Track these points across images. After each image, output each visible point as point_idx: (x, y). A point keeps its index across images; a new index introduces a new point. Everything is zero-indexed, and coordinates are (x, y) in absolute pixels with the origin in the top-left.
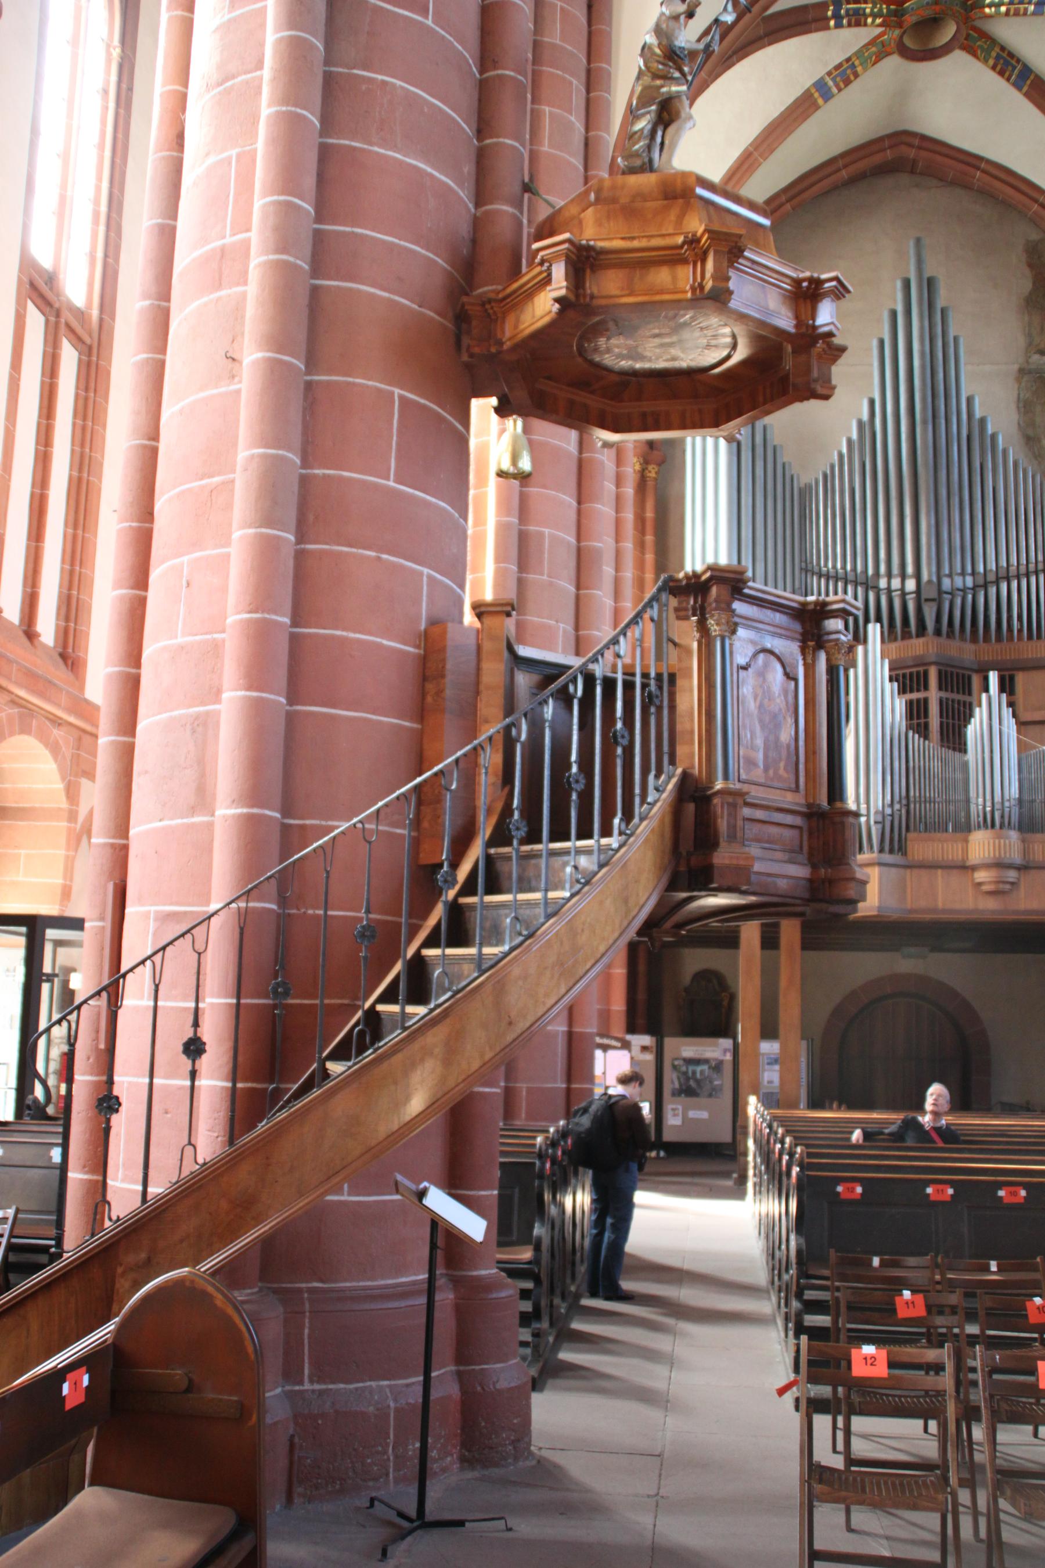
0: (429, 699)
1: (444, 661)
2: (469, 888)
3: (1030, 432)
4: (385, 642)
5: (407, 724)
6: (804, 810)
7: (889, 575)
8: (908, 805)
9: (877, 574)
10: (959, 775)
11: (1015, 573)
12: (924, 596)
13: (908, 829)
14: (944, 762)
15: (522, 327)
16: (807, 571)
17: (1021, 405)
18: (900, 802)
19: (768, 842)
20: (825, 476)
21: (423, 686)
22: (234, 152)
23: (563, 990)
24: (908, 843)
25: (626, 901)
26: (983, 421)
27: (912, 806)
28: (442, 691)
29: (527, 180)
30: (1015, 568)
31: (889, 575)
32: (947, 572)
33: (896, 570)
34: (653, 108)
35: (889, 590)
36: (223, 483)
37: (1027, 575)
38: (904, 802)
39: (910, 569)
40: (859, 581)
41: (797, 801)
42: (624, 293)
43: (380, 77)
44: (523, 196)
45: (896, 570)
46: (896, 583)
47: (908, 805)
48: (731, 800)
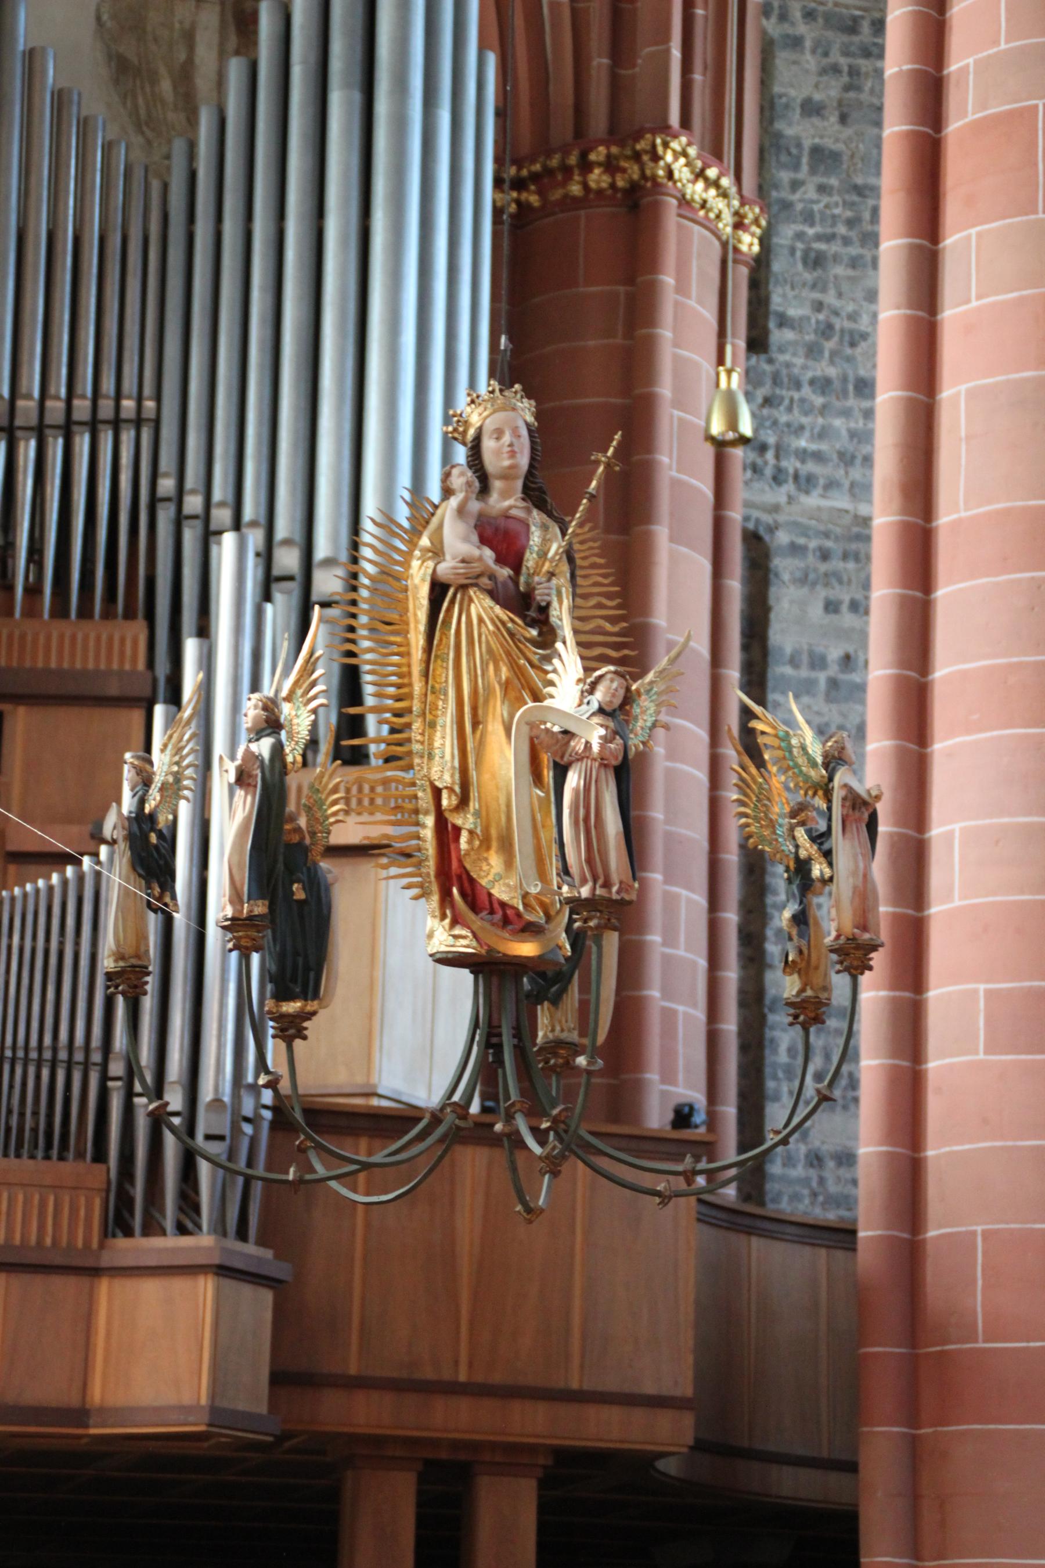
11: (34, 421)
30: (33, 405)
37: (68, 431)
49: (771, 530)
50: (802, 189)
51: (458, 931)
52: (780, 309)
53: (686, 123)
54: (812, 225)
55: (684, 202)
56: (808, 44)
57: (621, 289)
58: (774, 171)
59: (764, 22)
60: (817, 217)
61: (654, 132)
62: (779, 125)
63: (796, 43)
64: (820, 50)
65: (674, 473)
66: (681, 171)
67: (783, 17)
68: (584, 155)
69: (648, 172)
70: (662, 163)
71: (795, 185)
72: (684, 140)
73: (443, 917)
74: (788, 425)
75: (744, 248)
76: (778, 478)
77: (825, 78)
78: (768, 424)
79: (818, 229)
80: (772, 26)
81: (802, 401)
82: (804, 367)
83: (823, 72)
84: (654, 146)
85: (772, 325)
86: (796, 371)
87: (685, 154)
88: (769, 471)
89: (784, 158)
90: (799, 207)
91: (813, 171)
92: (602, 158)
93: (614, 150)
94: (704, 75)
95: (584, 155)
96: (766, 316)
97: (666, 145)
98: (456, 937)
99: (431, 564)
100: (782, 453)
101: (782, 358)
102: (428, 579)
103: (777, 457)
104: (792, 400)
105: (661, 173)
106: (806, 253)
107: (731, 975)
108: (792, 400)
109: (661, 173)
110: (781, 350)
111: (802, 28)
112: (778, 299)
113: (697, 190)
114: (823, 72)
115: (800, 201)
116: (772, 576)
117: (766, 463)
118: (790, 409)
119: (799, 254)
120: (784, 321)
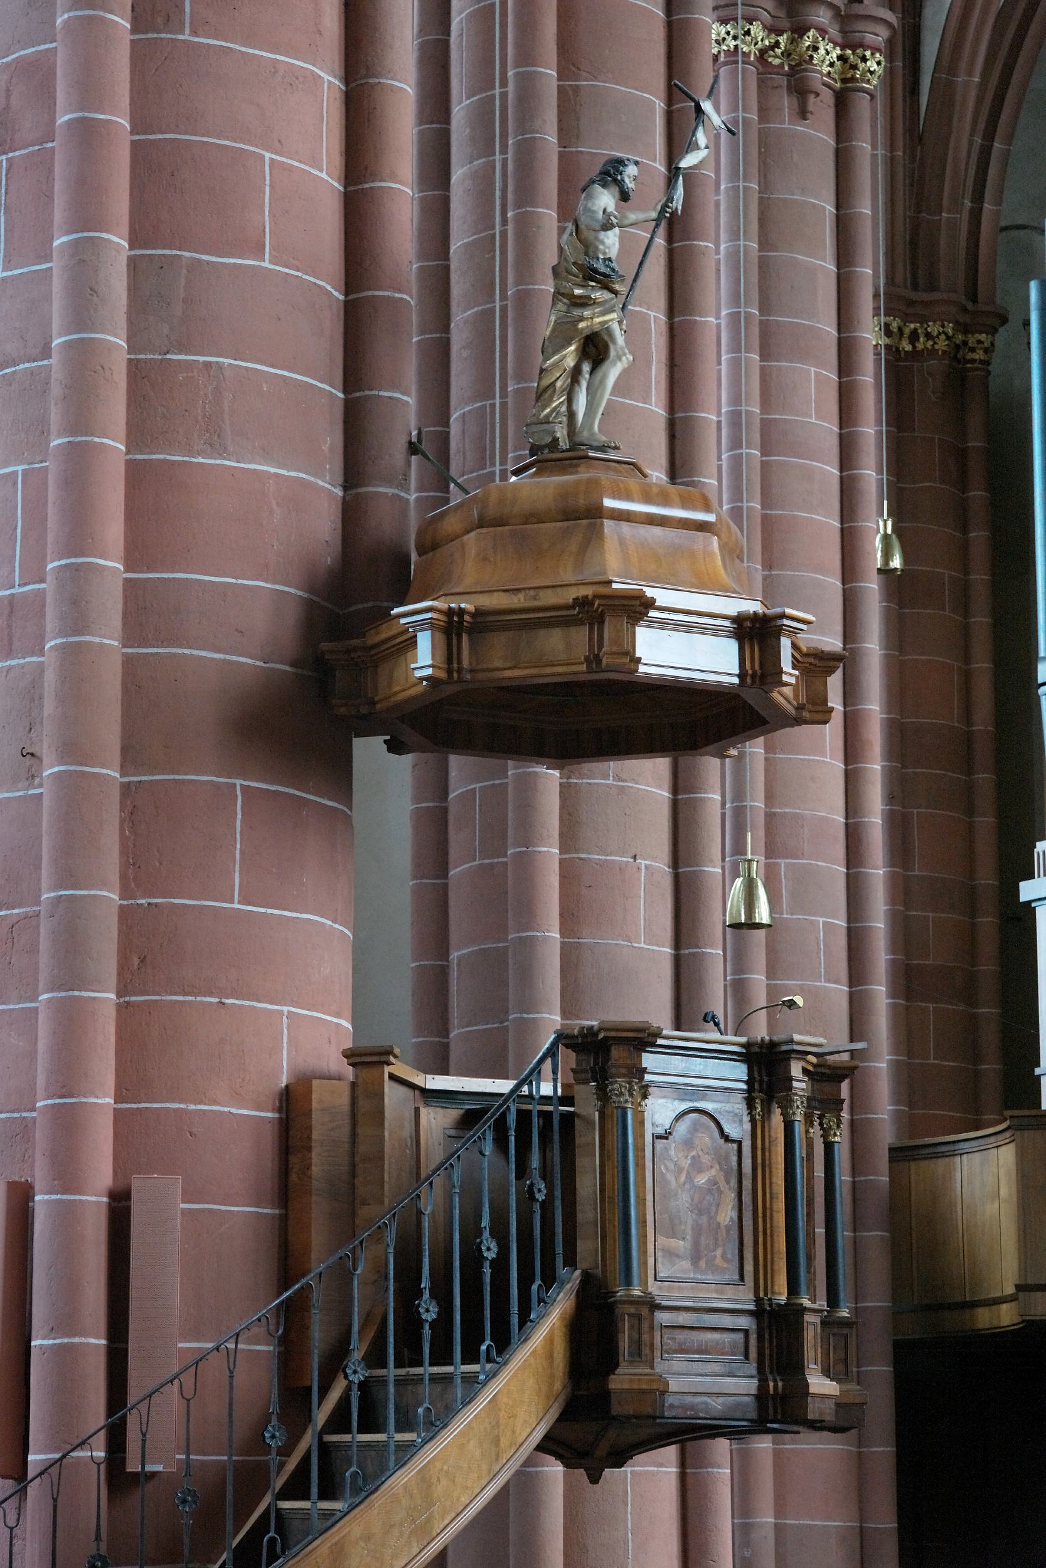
0: (294, 1177)
1: (309, 1128)
2: (339, 1421)
4: (234, 1111)
5: (265, 1211)
6: (752, 1307)
15: (396, 689)
19: (699, 1351)
21: (287, 1161)
22: (20, 468)
23: (415, 1550)
25: (497, 1441)
28: (309, 1167)
29: (414, 439)
34: (573, 348)
36: (26, 917)
41: (741, 1296)
42: (508, 665)
43: (201, 359)
44: (408, 464)
48: (632, 1310)
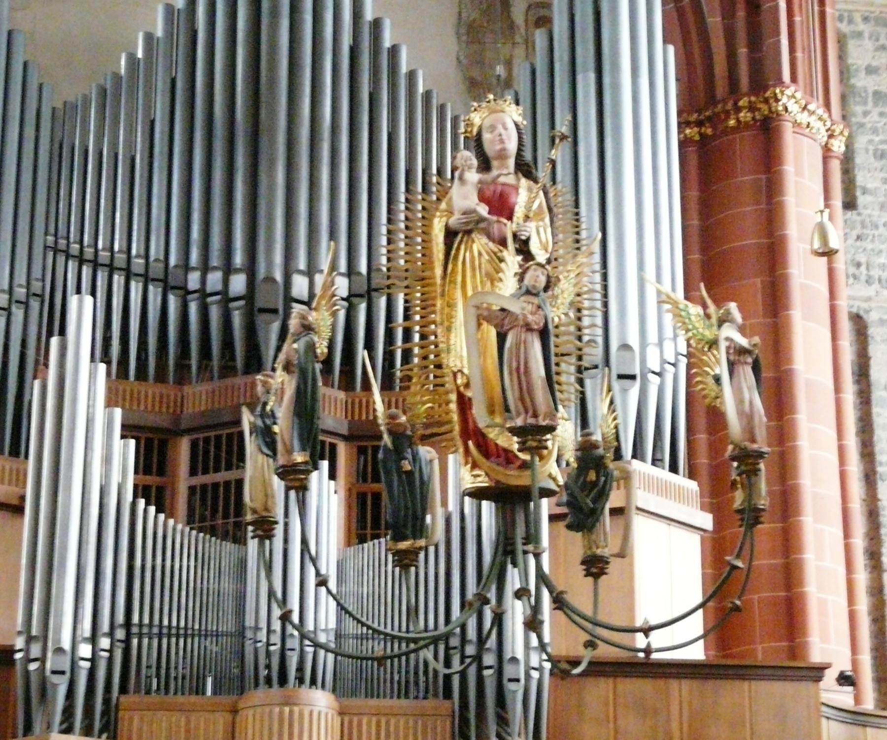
3: (476, 73)
7: (205, 268)
8: (127, 642)
9: (186, 267)
10: (228, 585)
12: (260, 303)
13: (123, 690)
14: (202, 562)
16: (56, 251)
17: (463, 31)
18: (111, 634)
20: (103, 92)
24: (121, 714)
26: (377, 24)
27: (135, 642)
31: (205, 268)
32: (302, 265)
33: (215, 260)
35: (203, 293)
38: (120, 634)
39: (239, 259)
40: (151, 275)
45: (215, 260)
46: (214, 279)
47: (127, 642)
49: (867, 312)
50: (870, 116)
51: (476, 472)
52: (863, 184)
53: (794, 79)
54: (878, 135)
55: (796, 124)
56: (866, 35)
57: (764, 176)
58: (852, 106)
59: (839, 25)
60: (881, 130)
61: (775, 86)
62: (853, 81)
63: (859, 35)
64: (874, 38)
65: (803, 281)
66: (793, 107)
67: (851, 21)
68: (736, 104)
69: (773, 109)
70: (780, 103)
71: (866, 114)
72: (793, 88)
73: (466, 463)
74: (873, 250)
75: (835, 149)
76: (869, 282)
77: (877, 53)
78: (860, 250)
79: (881, 137)
80: (844, 27)
81: (880, 236)
82: (879, 216)
83: (877, 49)
84: (775, 94)
85: (858, 193)
86: (875, 219)
87: (793, 97)
88: (863, 278)
89: (857, 99)
90: (869, 126)
91: (876, 104)
92: (746, 104)
93: (753, 99)
94: (803, 53)
95: (736, 104)
96: (855, 187)
97: (782, 92)
98: (476, 476)
99: (444, 219)
100: (870, 268)
101: (866, 212)
102: (443, 230)
103: (868, 269)
104: (874, 236)
105: (780, 108)
106: (876, 150)
107: (862, 578)
108: (874, 236)
109: (780, 108)
110: (865, 207)
111: (861, 27)
112: (861, 178)
113: (803, 118)
114: (877, 49)
115: (870, 122)
116: (870, 339)
117: (861, 274)
118: (873, 241)
119: (871, 152)
120: (865, 191)
